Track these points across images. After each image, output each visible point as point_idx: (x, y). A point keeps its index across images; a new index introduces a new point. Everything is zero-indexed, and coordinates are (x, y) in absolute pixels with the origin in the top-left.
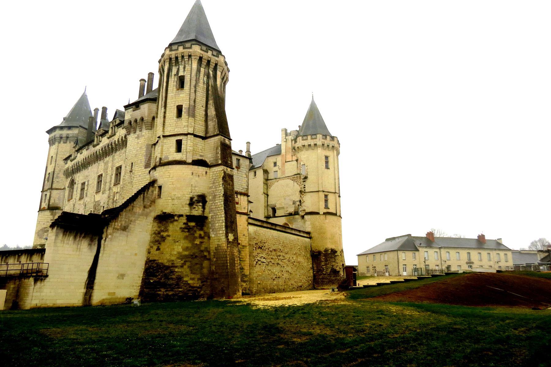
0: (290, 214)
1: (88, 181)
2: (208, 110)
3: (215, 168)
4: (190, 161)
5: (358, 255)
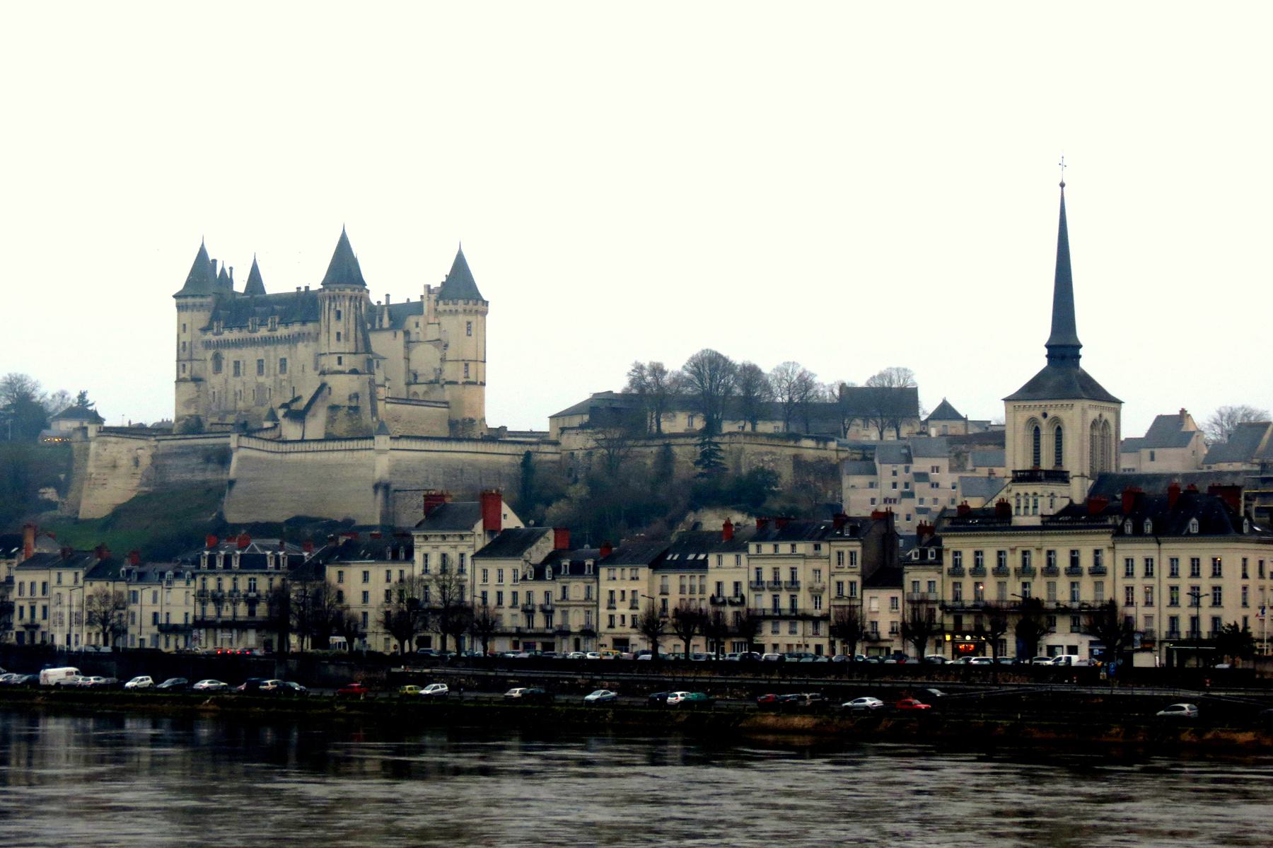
0: (431, 382)
1: (244, 361)
4: (347, 371)
5: (551, 417)
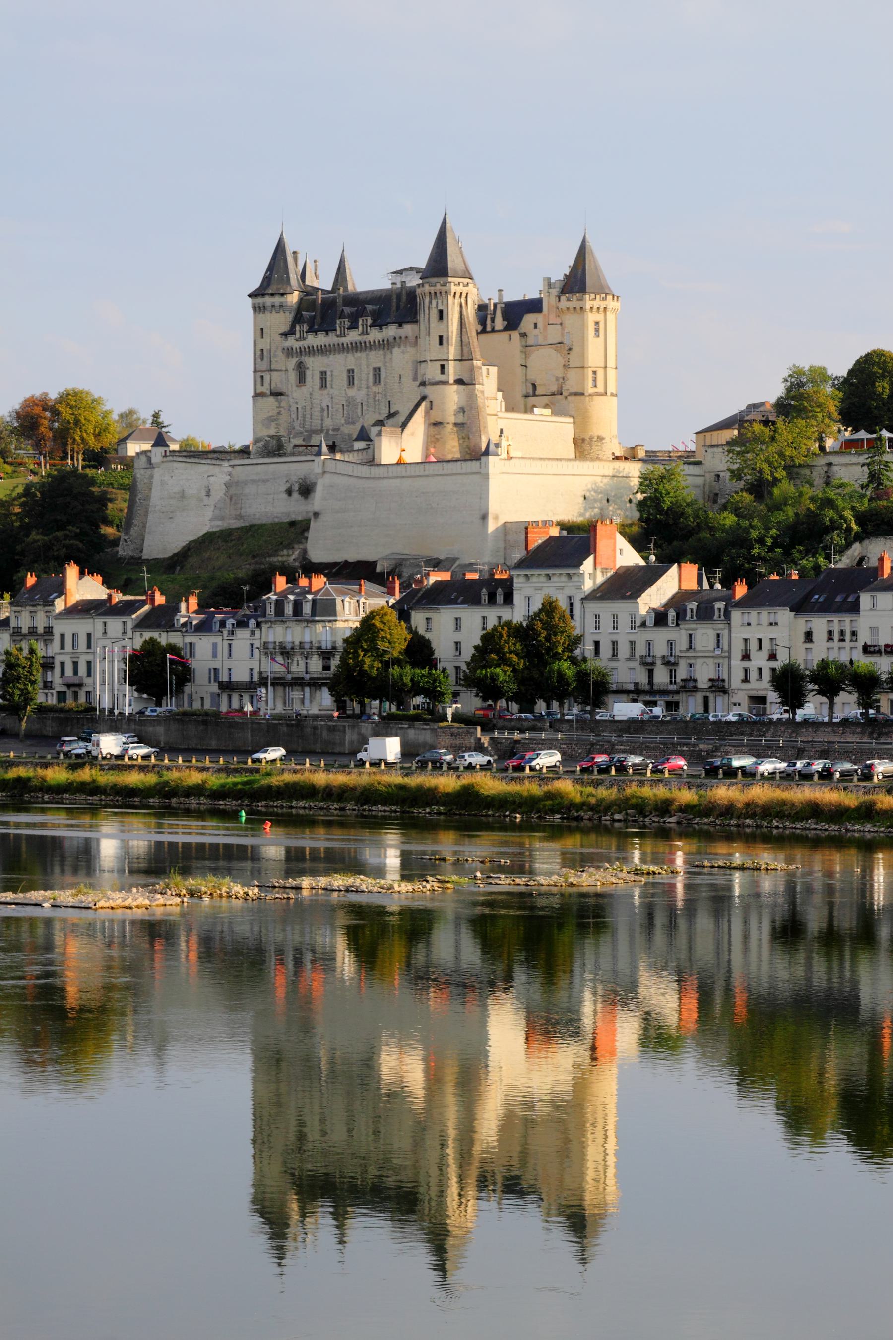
1: (332, 371)
5: (696, 433)
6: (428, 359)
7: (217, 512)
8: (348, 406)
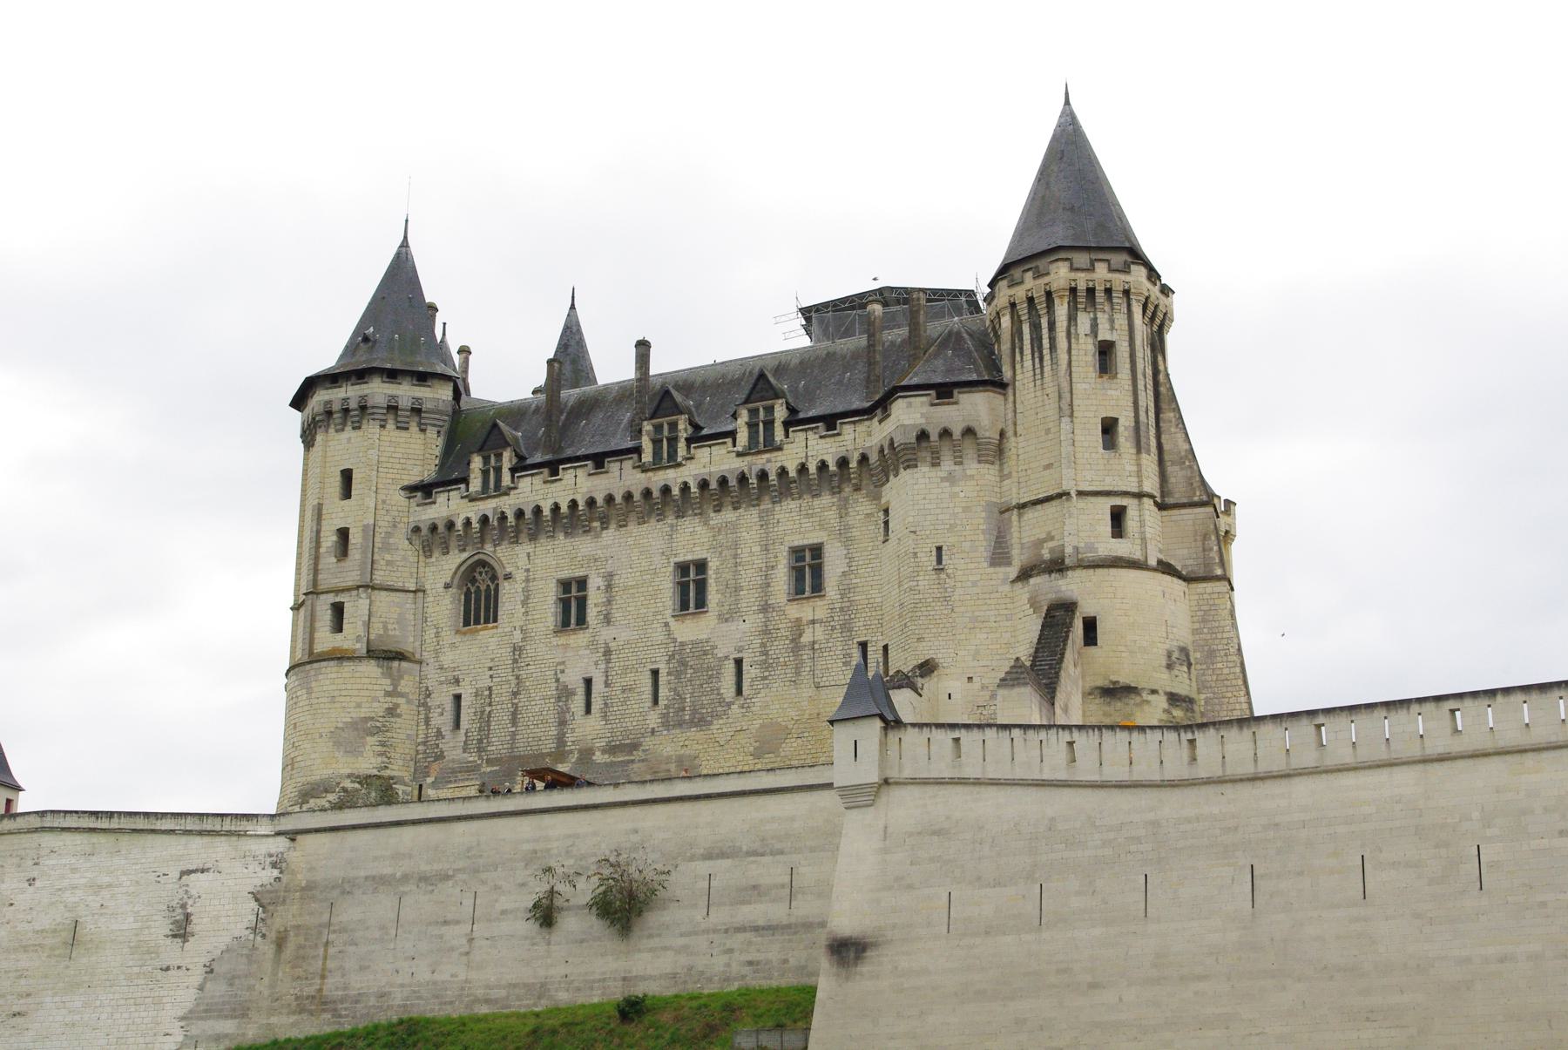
2: (1163, 436)
3: (1205, 585)
4: (1153, 562)
6: (1068, 485)
7: (217, 989)
8: (677, 674)
